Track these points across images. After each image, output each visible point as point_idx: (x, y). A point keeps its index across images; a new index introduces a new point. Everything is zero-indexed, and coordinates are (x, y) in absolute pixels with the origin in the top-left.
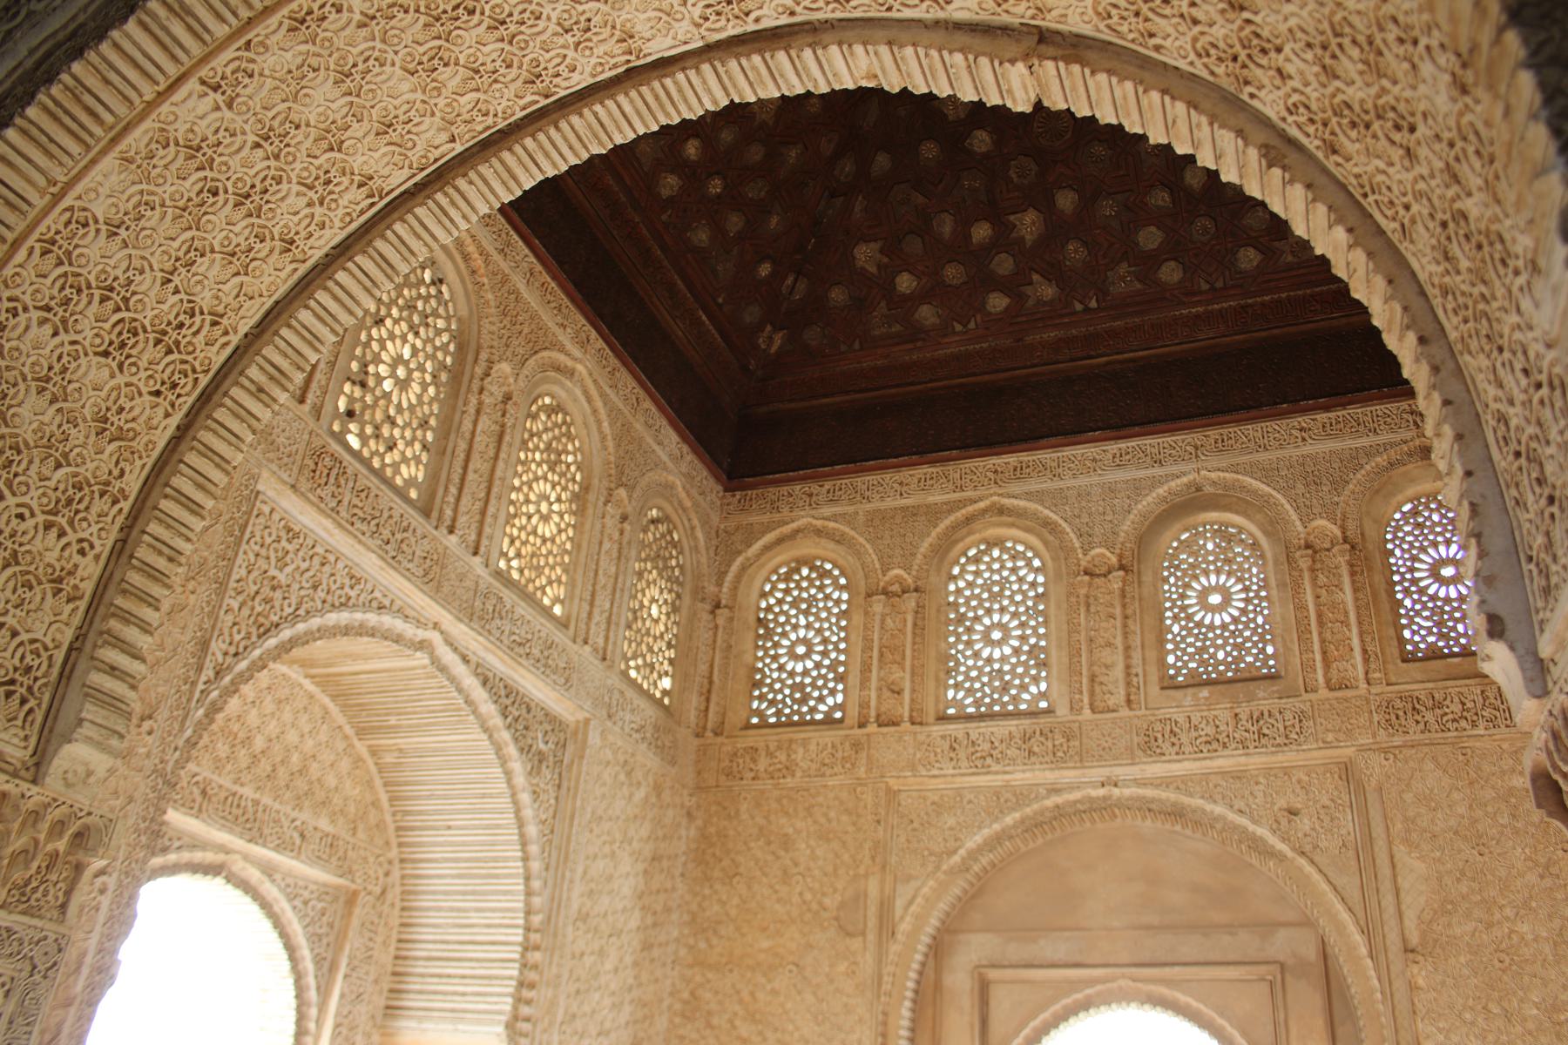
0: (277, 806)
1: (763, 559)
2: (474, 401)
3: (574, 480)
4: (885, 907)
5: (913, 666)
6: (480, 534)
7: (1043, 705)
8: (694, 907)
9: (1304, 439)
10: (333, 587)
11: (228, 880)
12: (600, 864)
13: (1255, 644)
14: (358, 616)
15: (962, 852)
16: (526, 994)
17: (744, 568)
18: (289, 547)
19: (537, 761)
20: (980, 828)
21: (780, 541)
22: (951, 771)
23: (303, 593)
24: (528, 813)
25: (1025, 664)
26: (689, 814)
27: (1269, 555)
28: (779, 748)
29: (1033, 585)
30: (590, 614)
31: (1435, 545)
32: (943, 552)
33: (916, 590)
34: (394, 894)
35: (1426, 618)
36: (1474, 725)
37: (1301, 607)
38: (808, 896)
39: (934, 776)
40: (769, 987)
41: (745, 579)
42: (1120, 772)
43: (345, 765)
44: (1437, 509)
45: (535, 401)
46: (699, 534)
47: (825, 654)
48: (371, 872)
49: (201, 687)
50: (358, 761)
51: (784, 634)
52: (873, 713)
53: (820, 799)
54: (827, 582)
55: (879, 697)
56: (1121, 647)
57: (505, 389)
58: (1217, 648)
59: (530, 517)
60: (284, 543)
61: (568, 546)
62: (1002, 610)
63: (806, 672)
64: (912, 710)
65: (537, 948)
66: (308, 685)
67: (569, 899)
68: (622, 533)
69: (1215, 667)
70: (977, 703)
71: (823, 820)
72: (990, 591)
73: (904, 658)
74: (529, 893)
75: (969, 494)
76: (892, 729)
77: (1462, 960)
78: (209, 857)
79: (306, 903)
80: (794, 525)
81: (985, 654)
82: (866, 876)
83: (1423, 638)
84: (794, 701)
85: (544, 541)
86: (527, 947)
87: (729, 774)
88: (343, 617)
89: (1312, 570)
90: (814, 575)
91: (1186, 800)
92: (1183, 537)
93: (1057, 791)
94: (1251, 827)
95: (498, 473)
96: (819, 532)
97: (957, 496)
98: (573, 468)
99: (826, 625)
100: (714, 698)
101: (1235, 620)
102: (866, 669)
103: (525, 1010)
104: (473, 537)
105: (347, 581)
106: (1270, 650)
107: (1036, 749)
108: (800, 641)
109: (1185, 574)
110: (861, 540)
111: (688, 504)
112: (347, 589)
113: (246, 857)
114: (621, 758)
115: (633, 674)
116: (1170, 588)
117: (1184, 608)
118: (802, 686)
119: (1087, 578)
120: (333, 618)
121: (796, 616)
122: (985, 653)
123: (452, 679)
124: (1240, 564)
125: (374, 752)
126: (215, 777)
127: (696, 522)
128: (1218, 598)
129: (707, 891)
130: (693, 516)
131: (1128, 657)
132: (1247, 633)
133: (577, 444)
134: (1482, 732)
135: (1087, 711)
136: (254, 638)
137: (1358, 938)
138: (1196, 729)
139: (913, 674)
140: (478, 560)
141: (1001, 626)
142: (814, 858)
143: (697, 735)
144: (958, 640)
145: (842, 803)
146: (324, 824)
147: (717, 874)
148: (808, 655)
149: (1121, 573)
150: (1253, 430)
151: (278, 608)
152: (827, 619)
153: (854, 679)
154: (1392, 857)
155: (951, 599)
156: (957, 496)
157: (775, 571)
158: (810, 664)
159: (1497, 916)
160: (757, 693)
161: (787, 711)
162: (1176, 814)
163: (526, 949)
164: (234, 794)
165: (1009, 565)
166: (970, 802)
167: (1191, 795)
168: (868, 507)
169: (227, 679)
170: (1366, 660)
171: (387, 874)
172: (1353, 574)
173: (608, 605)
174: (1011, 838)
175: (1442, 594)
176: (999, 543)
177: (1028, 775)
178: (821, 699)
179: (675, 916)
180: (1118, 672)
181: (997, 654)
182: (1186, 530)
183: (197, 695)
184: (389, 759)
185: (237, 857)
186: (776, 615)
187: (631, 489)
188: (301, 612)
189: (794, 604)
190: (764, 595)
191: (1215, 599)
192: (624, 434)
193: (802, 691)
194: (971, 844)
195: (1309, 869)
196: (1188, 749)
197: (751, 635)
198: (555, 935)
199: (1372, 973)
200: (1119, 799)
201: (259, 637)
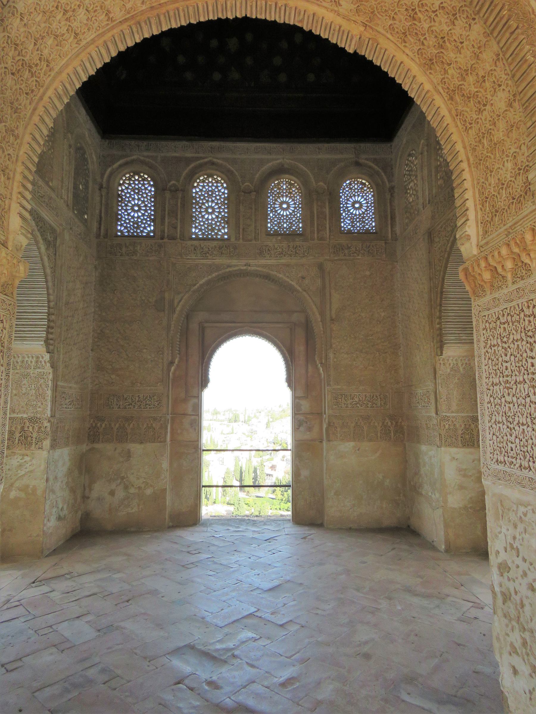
7: (226, 237)
15: (198, 285)
16: (50, 330)
21: (126, 164)
24: (47, 264)
26: (95, 267)
29: (224, 193)
30: (62, 186)
31: (354, 196)
32: (192, 176)
36: (358, 255)
37: (312, 213)
39: (189, 259)
42: (251, 261)
44: (357, 184)
47: (146, 211)
52: (166, 235)
54: (146, 183)
55: (168, 229)
56: (253, 220)
58: (284, 223)
62: (212, 201)
63: (138, 217)
64: (180, 235)
65: (53, 314)
68: (70, 152)
70: (203, 234)
72: (208, 194)
73: (177, 215)
74: (48, 294)
75: (201, 155)
81: (206, 216)
84: (134, 227)
86: (49, 314)
90: (140, 179)
91: (271, 272)
92: (276, 183)
94: (290, 282)
96: (142, 162)
101: (291, 214)
103: (51, 336)
106: (301, 225)
107: (224, 252)
109: (276, 196)
116: (270, 200)
117: (274, 208)
118: (137, 223)
119: (243, 193)
122: (206, 216)
128: (285, 207)
129: (104, 295)
131: (255, 223)
135: (241, 241)
137: (318, 316)
139: (181, 222)
143: (97, 238)
149: (255, 193)
150: (302, 147)
152: (146, 197)
156: (197, 155)
157: (124, 176)
158: (140, 214)
159: (357, 311)
160: (119, 223)
162: (267, 277)
163: (49, 315)
165: (215, 185)
167: (273, 271)
168: (162, 155)
170: (330, 232)
172: (329, 203)
176: (211, 176)
181: (210, 217)
182: (277, 180)
186: (126, 193)
187: (72, 134)
189: (133, 190)
190: (121, 185)
191: (285, 206)
195: (306, 295)
196: (273, 256)
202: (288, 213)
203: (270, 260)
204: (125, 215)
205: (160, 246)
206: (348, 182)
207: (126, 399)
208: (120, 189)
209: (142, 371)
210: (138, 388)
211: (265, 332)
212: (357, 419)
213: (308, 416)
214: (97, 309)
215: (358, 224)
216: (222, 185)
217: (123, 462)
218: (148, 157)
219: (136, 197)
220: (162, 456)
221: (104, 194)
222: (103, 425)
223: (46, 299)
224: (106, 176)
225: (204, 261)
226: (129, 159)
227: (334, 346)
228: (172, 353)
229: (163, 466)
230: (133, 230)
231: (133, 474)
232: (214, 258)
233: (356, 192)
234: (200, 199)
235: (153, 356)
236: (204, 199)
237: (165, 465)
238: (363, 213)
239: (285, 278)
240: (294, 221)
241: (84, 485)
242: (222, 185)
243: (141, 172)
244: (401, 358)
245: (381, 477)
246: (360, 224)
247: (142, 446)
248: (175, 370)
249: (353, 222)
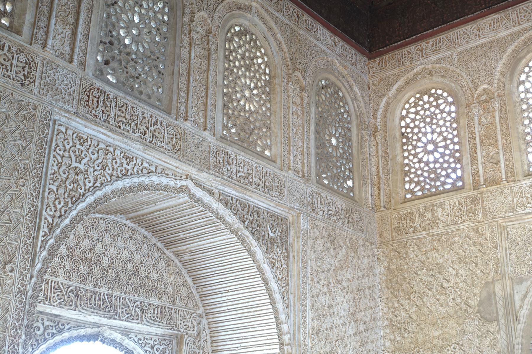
0: (123, 295)
1: (399, 96)
2: (186, 39)
3: (265, 73)
4: (509, 300)
6: (205, 118)
8: (390, 316)
10: (116, 166)
11: (103, 341)
12: (322, 299)
14: (136, 180)
17: (388, 105)
18: (82, 148)
19: (270, 245)
23: (96, 173)
28: (426, 210)
30: (289, 151)
32: (513, 67)
33: (498, 96)
34: (206, 334)
38: (459, 300)
41: (389, 111)
43: (161, 265)
45: (229, 31)
46: (356, 90)
47: (446, 147)
48: (189, 324)
49: (41, 238)
50: (169, 261)
51: (419, 140)
52: (482, 179)
53: (456, 239)
55: (484, 168)
57: (205, 28)
59: (239, 101)
60: (78, 146)
61: (268, 114)
63: (436, 161)
64: (506, 173)
66: (128, 223)
67: (304, 322)
68: (302, 98)
71: (460, 251)
73: (496, 141)
78: (89, 331)
79: (152, 348)
80: (415, 71)
82: (493, 282)
85: (251, 113)
87: (398, 231)
88: (127, 182)
90: (432, 99)
95: (211, 78)
96: (430, 73)
97: (516, 29)
98: (263, 67)
99: (444, 129)
100: (382, 187)
104: (202, 120)
105: (124, 161)
108: (429, 142)
110: (459, 71)
111: (345, 72)
112: (125, 166)
113: (111, 327)
114: (326, 234)
115: (326, 182)
118: (434, 171)
120: (119, 184)
121: (425, 127)
123: (206, 206)
125: (178, 255)
126: (82, 286)
127: (352, 82)
129: (396, 305)
130: (350, 79)
133: (263, 51)
136: (70, 205)
139: (504, 149)
140: (206, 134)
142: (458, 276)
145: (470, 239)
146: (154, 301)
147: (400, 293)
148: (435, 150)
151: (82, 185)
153: (466, 159)
155: (522, 96)
156: (516, 29)
158: (437, 155)
161: (428, 187)
164: (95, 294)
168: (459, 49)
169: (58, 231)
171: (199, 324)
173: (300, 144)
178: (448, 176)
179: (379, 323)
183: (39, 244)
184: (186, 258)
185: (106, 328)
186: (412, 129)
187: (303, 71)
188: (98, 184)
190: (403, 118)
192: (293, 39)
193: (435, 173)
197: (398, 145)
198: (299, 346)
201: (73, 204)
204: (414, 163)
205: (474, 201)
214: (388, 331)
218: (439, 61)
219: (429, 130)
221: (379, 139)
223: (275, 330)
224: (380, 112)
226: (410, 75)
230: (430, 184)
243: (431, 89)
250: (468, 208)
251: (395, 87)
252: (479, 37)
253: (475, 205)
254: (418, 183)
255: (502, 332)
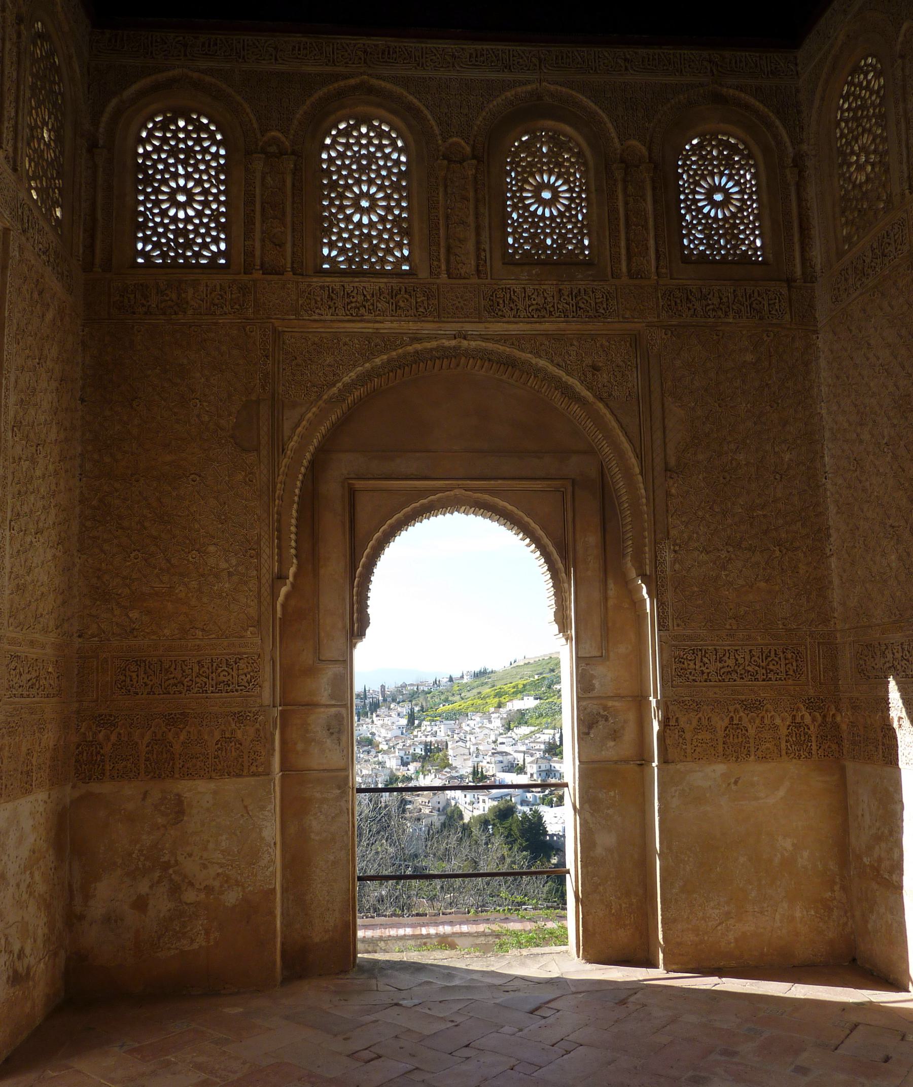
5: (293, 222)
7: (405, 268)
9: (626, 69)
13: (575, 236)
15: (339, 385)
20: (355, 366)
22: (329, 317)
25: (389, 231)
27: (591, 164)
29: (397, 162)
31: (712, 175)
33: (293, 153)
35: (700, 232)
36: (726, 315)
38: (206, 418)
40: (174, 494)
42: (468, 327)
44: (716, 147)
47: (206, 204)
51: (164, 182)
52: (258, 262)
55: (263, 247)
56: (473, 225)
62: (370, 182)
63: (188, 219)
64: (293, 263)
69: (544, 252)
70: (350, 261)
76: (275, 277)
77: (701, 477)
80: (171, 74)
81: (356, 218)
83: (696, 247)
89: (625, 181)
91: (517, 353)
92: (524, 139)
93: (416, 339)
94: (565, 377)
102: (249, 222)
106: (586, 242)
107: (401, 304)
109: (524, 171)
110: (239, 98)
117: (523, 199)
118: (184, 233)
119: (445, 162)
122: (356, 218)
124: (568, 168)
131: (478, 234)
132: (570, 227)
134: (731, 320)
137: (633, 461)
138: (530, 299)
139: (293, 230)
141: (367, 196)
144: (332, 204)
149: (474, 162)
152: (206, 171)
154: (663, 405)
158: (191, 213)
160: (140, 235)
162: (510, 363)
165: (376, 142)
166: (345, 344)
167: (523, 350)
170: (658, 258)
172: (654, 189)
174: (379, 376)
175: (712, 214)
177: (395, 325)
178: (205, 246)
180: (471, 245)
181: (365, 220)
186: (155, 162)
189: (174, 152)
190: (143, 142)
191: (547, 195)
194: (346, 379)
196: (523, 314)
199: (641, 486)
200: (466, 350)
202: (555, 213)
203: (516, 323)
206: (695, 142)
207: (167, 671)
208: (141, 151)
209: (205, 600)
210: (198, 642)
211: (502, 503)
212: (731, 708)
213: (610, 704)
214: (90, 448)
215: (722, 242)
216: (393, 144)
217: (164, 826)
219: (181, 171)
220: (262, 808)
222: (113, 738)
225: (357, 327)
227: (674, 532)
228: (280, 555)
229: (266, 834)
231: (190, 855)
232: (378, 318)
233: (715, 166)
234: (341, 176)
235: (234, 562)
236: (349, 175)
237: (271, 830)
238: (734, 216)
239: (552, 369)
240: (571, 231)
241: (70, 886)
242: (393, 144)
244: (833, 562)
245: (790, 848)
246: (727, 242)
247: (212, 785)
248: (288, 596)
249: (708, 237)
250: (234, 296)
251: (135, 88)
252: (276, 59)
253: (244, 295)
254: (157, 245)
255: (262, 467)
